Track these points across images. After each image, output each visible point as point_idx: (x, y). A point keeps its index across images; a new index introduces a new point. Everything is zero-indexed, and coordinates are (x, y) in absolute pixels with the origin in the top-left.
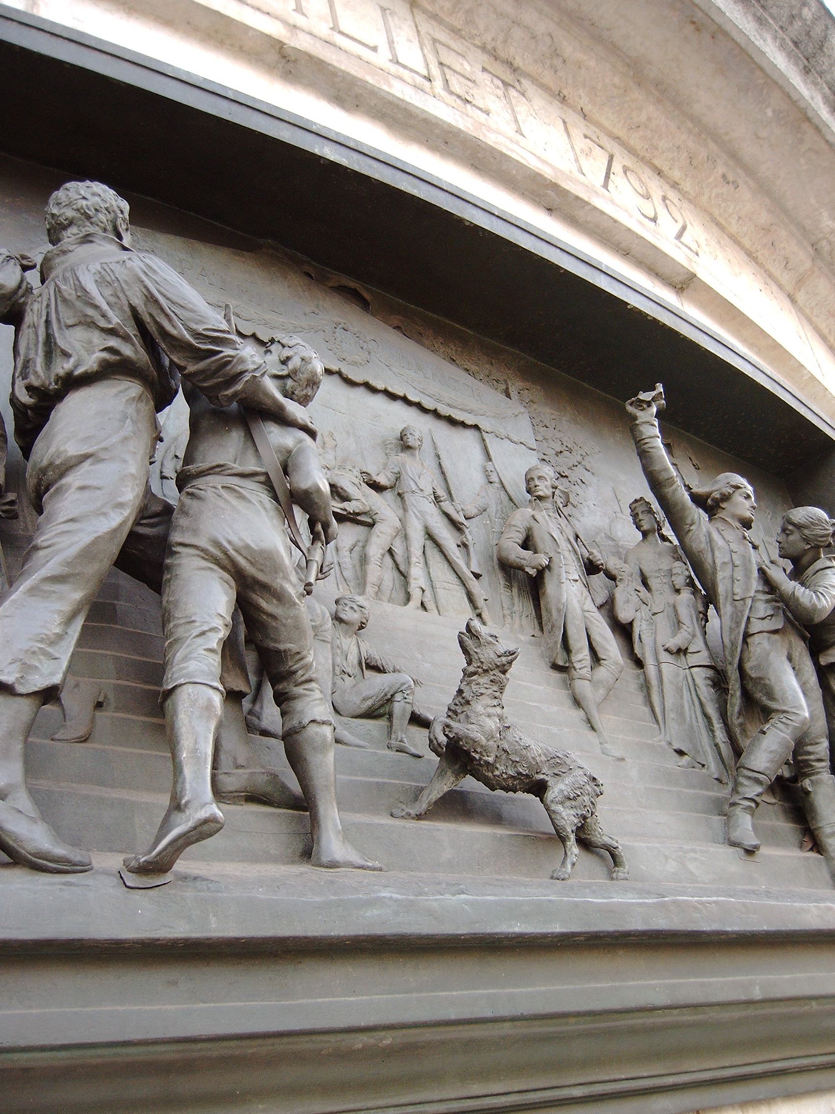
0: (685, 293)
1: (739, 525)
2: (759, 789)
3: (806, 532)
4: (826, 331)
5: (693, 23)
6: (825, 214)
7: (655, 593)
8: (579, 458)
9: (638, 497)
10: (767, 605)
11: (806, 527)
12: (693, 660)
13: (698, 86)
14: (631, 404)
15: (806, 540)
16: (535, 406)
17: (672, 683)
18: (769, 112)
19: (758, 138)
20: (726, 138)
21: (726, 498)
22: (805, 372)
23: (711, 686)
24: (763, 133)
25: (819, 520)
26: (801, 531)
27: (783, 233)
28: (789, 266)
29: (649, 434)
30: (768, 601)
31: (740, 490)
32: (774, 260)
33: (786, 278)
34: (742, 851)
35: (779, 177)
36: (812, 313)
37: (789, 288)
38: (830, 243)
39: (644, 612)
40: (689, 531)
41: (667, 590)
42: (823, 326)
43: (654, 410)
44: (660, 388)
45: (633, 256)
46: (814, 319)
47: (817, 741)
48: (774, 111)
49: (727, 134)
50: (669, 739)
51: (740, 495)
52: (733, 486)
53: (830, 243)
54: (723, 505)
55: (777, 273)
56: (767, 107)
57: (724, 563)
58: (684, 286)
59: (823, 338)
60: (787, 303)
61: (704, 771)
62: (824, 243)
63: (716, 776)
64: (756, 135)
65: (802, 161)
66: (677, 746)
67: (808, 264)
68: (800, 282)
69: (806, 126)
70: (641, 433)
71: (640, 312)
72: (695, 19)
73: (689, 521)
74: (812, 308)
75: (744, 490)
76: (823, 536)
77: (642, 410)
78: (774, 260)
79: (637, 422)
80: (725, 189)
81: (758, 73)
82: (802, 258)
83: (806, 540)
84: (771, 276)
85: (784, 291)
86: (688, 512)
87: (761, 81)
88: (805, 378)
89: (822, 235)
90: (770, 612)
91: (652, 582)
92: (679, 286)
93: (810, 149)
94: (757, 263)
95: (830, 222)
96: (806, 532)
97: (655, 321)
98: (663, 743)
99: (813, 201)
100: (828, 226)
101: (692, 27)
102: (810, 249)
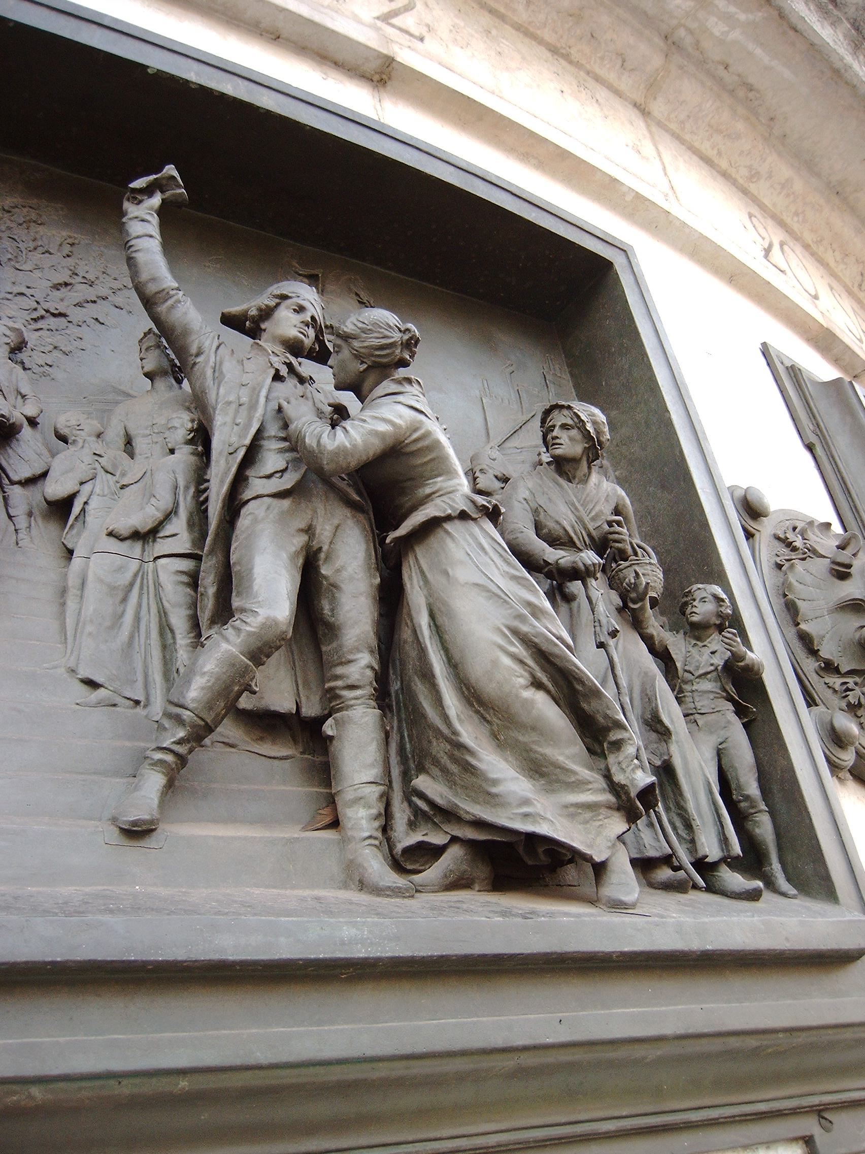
0: (388, 88)
1: (279, 349)
2: (181, 734)
3: (356, 344)
4: (712, 153)
7: (138, 457)
8: (104, 292)
9: (147, 330)
10: (278, 456)
11: (355, 337)
12: (162, 546)
14: (128, 200)
15: (358, 357)
16: (41, 229)
17: (101, 581)
21: (267, 313)
22: (624, 189)
23: (188, 585)
25: (375, 324)
26: (349, 344)
27: (605, 19)
29: (134, 235)
30: (281, 451)
31: (289, 302)
32: (602, 59)
33: (625, 83)
34: (117, 831)
36: (683, 129)
37: (638, 97)
38: (690, 32)
39: (104, 483)
40: (195, 364)
41: (157, 449)
42: (706, 147)
43: (156, 200)
44: (170, 170)
45: (288, 40)
46: (687, 137)
47: (351, 657)
50: (72, 664)
51: (287, 308)
52: (276, 296)
53: (690, 32)
54: (263, 326)
55: (612, 77)
57: (229, 403)
58: (384, 77)
59: (707, 161)
60: (634, 114)
61: (139, 710)
62: (682, 32)
63: (156, 719)
66: (84, 673)
67: (657, 61)
68: (653, 87)
70: (128, 234)
71: (173, 79)
73: (194, 350)
74: (682, 122)
75: (295, 300)
76: (382, 347)
77: (138, 204)
78: (602, 59)
79: (124, 220)
82: (648, 53)
83: (358, 357)
84: (598, 79)
85: (626, 100)
86: (193, 337)
88: (629, 198)
89: (674, 22)
90: (281, 465)
91: (140, 444)
92: (376, 78)
94: (571, 62)
96: (356, 344)
97: (204, 90)
98: (62, 671)
100: (678, 7)
102: (657, 40)
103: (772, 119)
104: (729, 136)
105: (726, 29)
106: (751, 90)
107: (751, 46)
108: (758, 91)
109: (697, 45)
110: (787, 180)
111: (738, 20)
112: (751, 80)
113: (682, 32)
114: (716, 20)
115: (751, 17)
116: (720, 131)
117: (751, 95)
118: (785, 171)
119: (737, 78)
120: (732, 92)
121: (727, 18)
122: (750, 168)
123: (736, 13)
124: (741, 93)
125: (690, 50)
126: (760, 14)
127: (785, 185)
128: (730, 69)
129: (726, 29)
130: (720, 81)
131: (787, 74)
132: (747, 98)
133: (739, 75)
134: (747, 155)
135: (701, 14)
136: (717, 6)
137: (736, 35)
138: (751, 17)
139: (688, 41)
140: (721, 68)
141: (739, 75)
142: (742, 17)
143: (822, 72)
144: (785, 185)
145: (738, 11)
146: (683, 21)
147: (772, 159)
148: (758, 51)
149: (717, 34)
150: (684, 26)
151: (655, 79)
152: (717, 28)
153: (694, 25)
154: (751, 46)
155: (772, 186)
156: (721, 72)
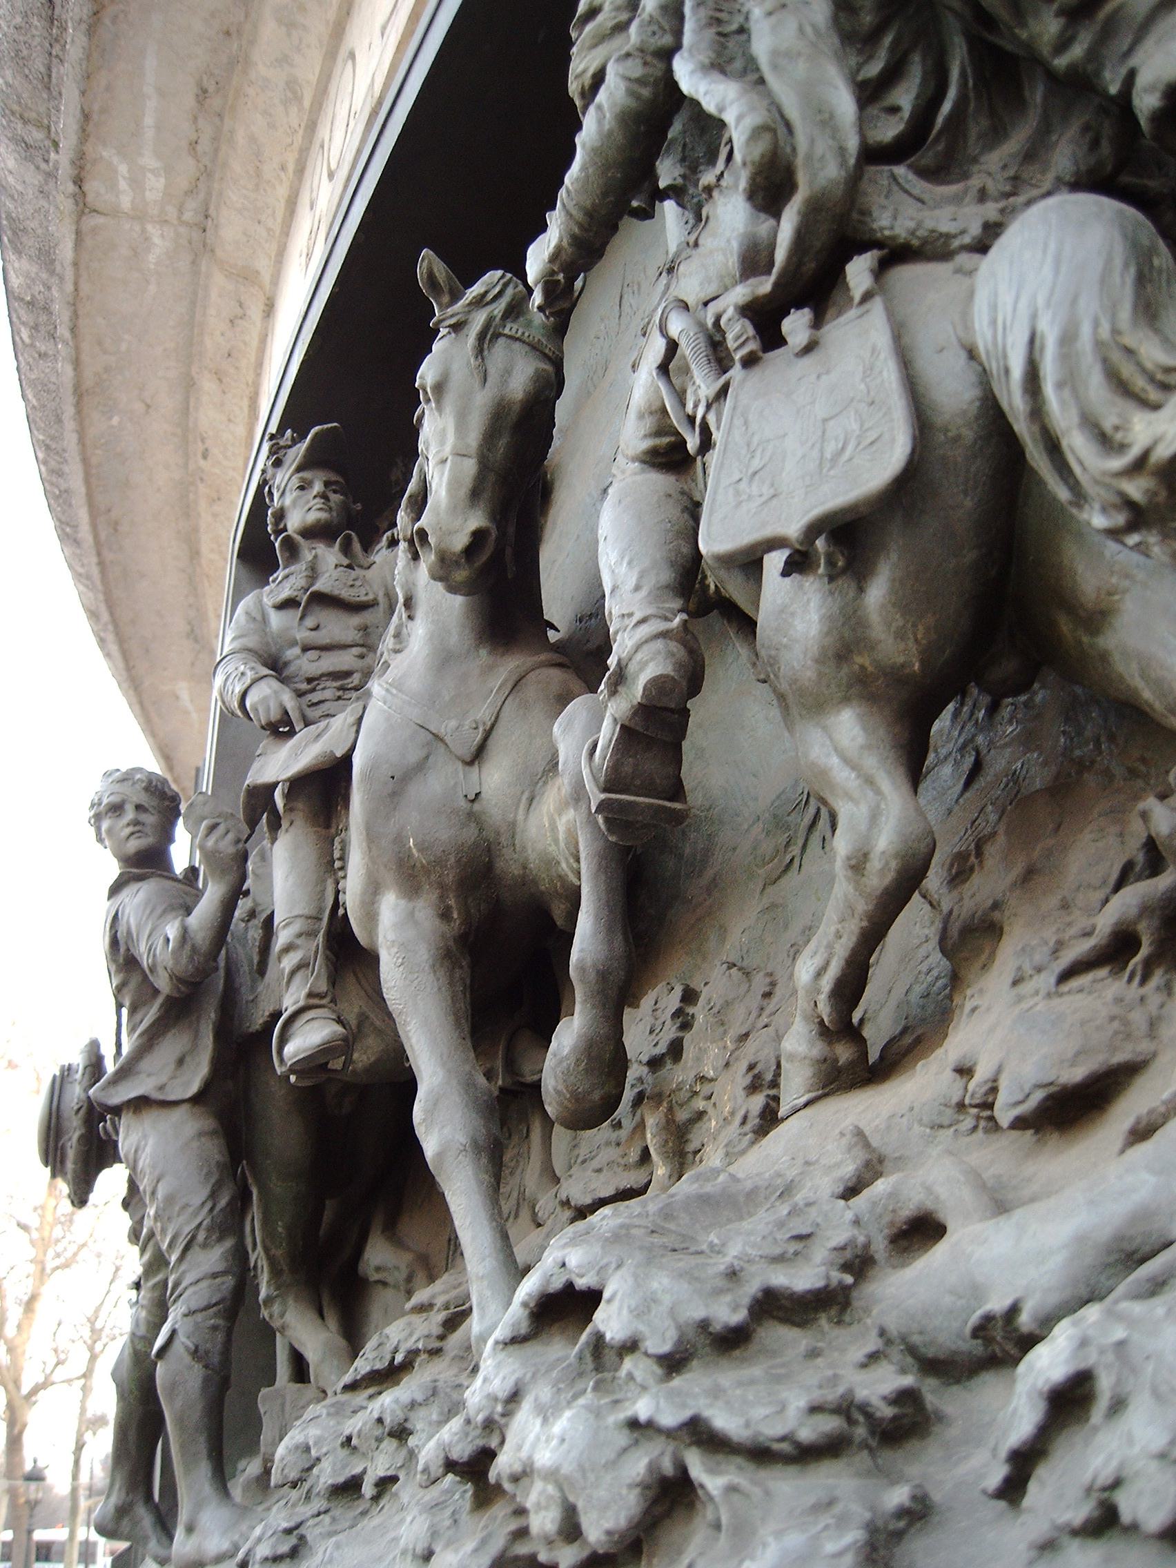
6: (152, 258)
13: (159, 490)
18: (115, 421)
19: (148, 406)
20: (179, 431)
24: (139, 407)
28: (239, 312)
32: (245, 343)
35: (165, 350)
38: (180, 212)
48: (110, 418)
49: (174, 434)
53: (180, 212)
56: (113, 427)
62: (188, 216)
64: (147, 412)
65: (124, 347)
69: (89, 382)
80: (215, 451)
81: (94, 461)
85: (266, 328)
87: (98, 452)
89: (182, 230)
93: (105, 352)
95: (157, 240)
99: (152, 288)
100: (162, 236)
103: (228, 33)
105: (149, 175)
106: (205, 91)
107: (149, 134)
109: (190, 192)
112: (189, 101)
114: (147, 193)
115: (115, 160)
116: (258, 173)
118: (269, 31)
119: (201, 122)
121: (136, 183)
122: (286, 103)
123: (124, 178)
124: (215, 102)
125: (202, 196)
126: (104, 154)
128: (194, 137)
129: (149, 175)
130: (216, 139)
131: (150, 63)
132: (218, 91)
133: (195, 119)
134: (270, 115)
136: (132, 202)
137: (149, 160)
138: (115, 160)
139: (192, 205)
140: (199, 148)
141: (195, 119)
142: (123, 169)
143: (114, 19)
146: (176, 222)
147: (262, 68)
148: (149, 121)
149: (162, 180)
150: (179, 218)
152: (155, 186)
153: (172, 212)
154: (149, 134)
155: (299, 49)
156: (205, 145)
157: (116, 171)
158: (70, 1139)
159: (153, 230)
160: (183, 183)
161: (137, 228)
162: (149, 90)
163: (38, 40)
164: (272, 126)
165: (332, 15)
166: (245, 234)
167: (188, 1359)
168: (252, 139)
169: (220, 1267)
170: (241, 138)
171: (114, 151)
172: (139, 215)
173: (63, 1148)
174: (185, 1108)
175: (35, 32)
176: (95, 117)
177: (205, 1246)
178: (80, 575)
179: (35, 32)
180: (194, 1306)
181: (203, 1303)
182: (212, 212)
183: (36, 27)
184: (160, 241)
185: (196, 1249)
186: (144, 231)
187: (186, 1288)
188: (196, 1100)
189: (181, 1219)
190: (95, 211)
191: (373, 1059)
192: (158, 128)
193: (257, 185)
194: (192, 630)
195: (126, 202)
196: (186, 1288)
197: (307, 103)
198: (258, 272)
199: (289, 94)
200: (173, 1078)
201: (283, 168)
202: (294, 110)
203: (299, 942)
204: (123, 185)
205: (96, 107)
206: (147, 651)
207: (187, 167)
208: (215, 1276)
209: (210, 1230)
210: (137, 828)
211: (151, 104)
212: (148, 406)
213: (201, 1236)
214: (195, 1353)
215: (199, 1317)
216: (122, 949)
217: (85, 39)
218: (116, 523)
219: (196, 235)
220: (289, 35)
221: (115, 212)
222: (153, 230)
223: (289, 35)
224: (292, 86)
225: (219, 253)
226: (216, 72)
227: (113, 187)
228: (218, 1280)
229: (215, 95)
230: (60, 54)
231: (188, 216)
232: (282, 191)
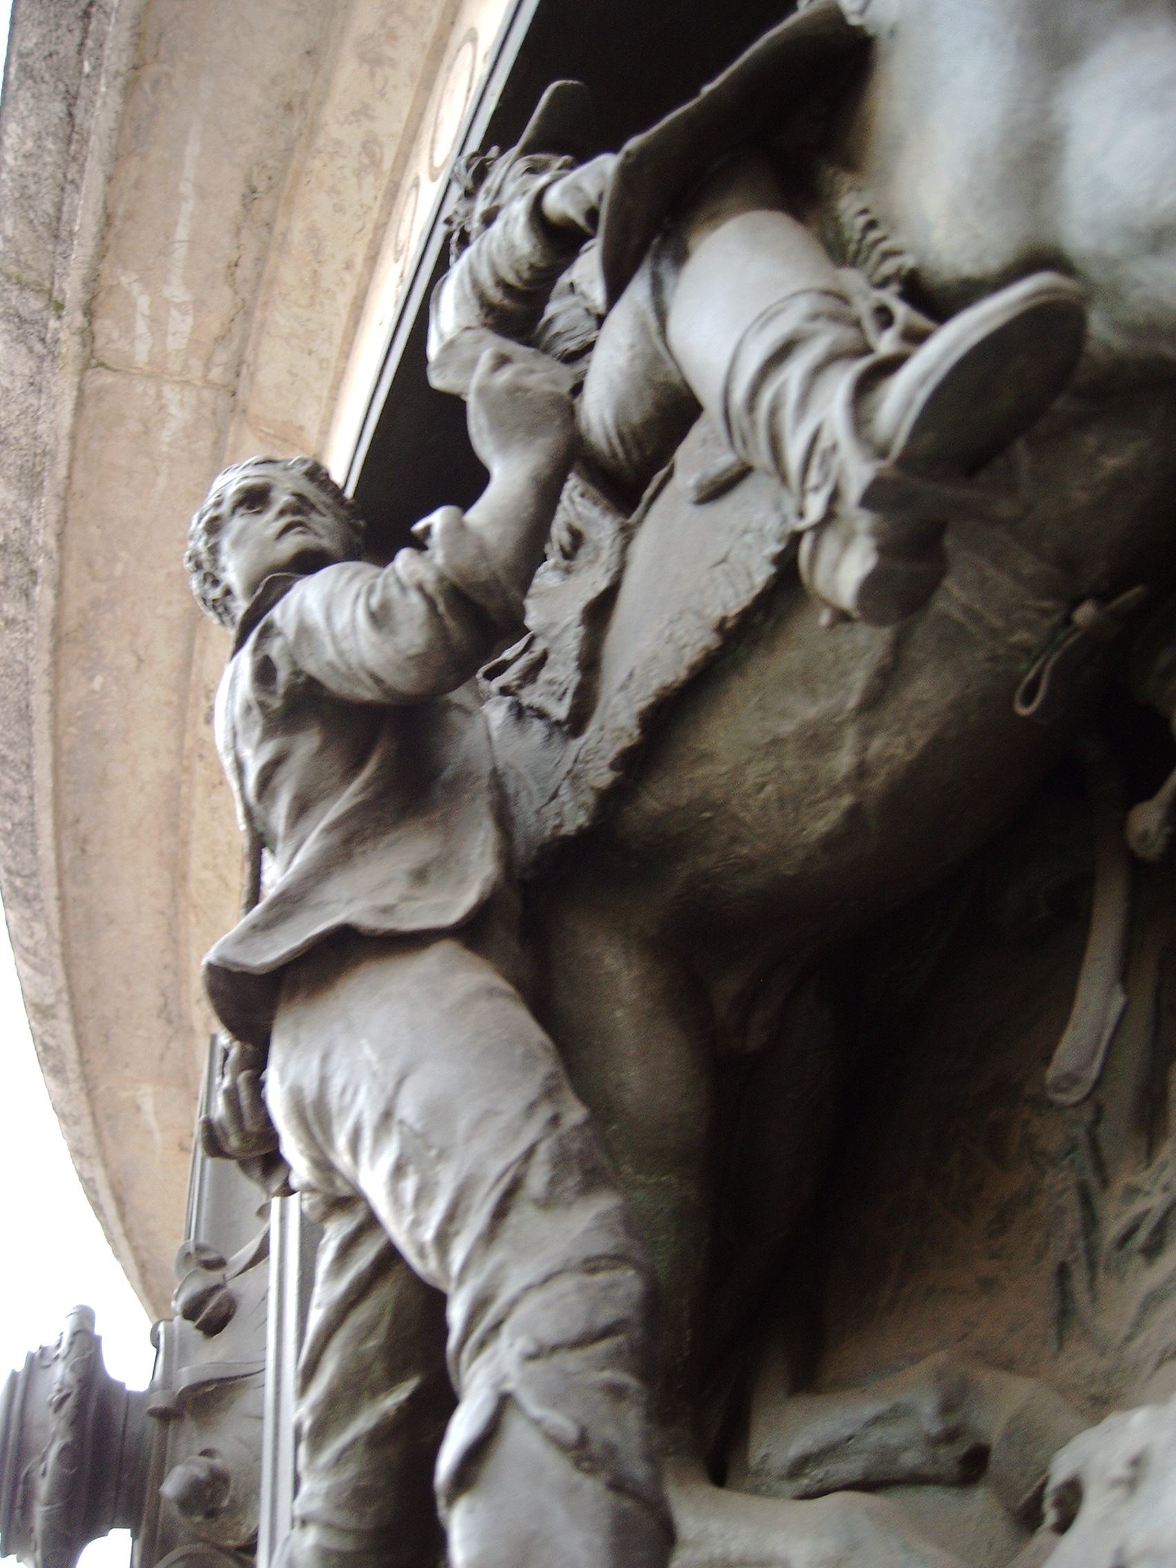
5: (83, 851)
6: (165, 436)
13: (142, 789)
18: (98, 683)
20: (175, 698)
24: (129, 661)
35: (169, 575)
38: (207, 368)
48: (91, 679)
49: (168, 703)
53: (207, 368)
56: (93, 692)
64: (138, 670)
65: (119, 569)
69: (70, 624)
72: (78, 852)
81: (66, 744)
87: (73, 730)
89: (207, 394)
93: (94, 579)
95: (173, 409)
99: (162, 481)
100: (182, 404)
101: (88, 848)
103: (289, 107)
104: (317, 253)
105: (174, 312)
107: (181, 252)
108: (248, 179)
109: (221, 339)
110: (362, 58)
111: (151, 306)
112: (233, 204)
113: (216, 374)
114: (170, 339)
115: (136, 289)
117: (262, 186)
118: (348, 75)
119: (244, 232)
120: (269, 225)
121: (157, 324)
122: (359, 173)
123: (144, 316)
124: (264, 206)
125: (235, 344)
127: (373, 60)
129: (174, 312)
130: (261, 260)
131: (193, 149)
132: (270, 188)
134: (338, 193)
135: (174, 366)
136: (150, 352)
137: (177, 292)
138: (136, 289)
139: (222, 357)
140: (239, 273)
142: (143, 302)
143: (156, 84)
144: (373, 60)
145: (139, 317)
146: (199, 383)
147: (336, 127)
148: (182, 233)
149: (190, 320)
150: (205, 376)
151: (276, 437)
152: (181, 325)
153: (196, 364)
154: (181, 252)
155: (382, 94)
156: (246, 270)
157: (134, 306)
158: (43, 1459)
159: (171, 394)
160: (215, 326)
161: (152, 392)
162: (186, 188)
163: (50, 169)
164: (339, 209)
165: (429, 33)
166: (290, 373)
167: (557, 1467)
168: (313, 231)
169: (602, 1244)
170: (297, 234)
171: (134, 276)
172: (157, 373)
173: (28, 1481)
174: (444, 951)
175: (49, 159)
176: (117, 223)
177: (547, 1203)
178: (27, 950)
179: (49, 159)
180: (549, 1331)
181: (575, 1329)
182: (249, 356)
183: (50, 152)
184: (178, 408)
185: (524, 1216)
186: (159, 396)
187: (514, 1303)
188: (471, 932)
189: (480, 1146)
190: (102, 364)
191: (920, 744)
192: (192, 243)
193: (312, 297)
194: (166, 1005)
195: (142, 352)
196: (514, 1303)
197: (387, 165)
198: (301, 428)
199: (366, 161)
200: (406, 898)
201: (348, 266)
202: (369, 179)
203: (819, 325)
204: (141, 327)
205: (120, 210)
206: (107, 1036)
207: (223, 299)
208: (591, 1265)
209: (561, 1161)
210: (298, 518)
211: (188, 207)
212: (140, 661)
213: (537, 1181)
214: (582, 1451)
215: (572, 1361)
216: (283, 675)
217: (119, 100)
218: (85, 840)
219: (223, 402)
220: (372, 75)
221: (124, 369)
222: (171, 394)
223: (372, 75)
224: (370, 146)
225: (255, 409)
226: (270, 163)
227: (128, 331)
228: (601, 1278)
229: (264, 198)
230: (77, 176)
231: (216, 374)
232: (344, 300)
